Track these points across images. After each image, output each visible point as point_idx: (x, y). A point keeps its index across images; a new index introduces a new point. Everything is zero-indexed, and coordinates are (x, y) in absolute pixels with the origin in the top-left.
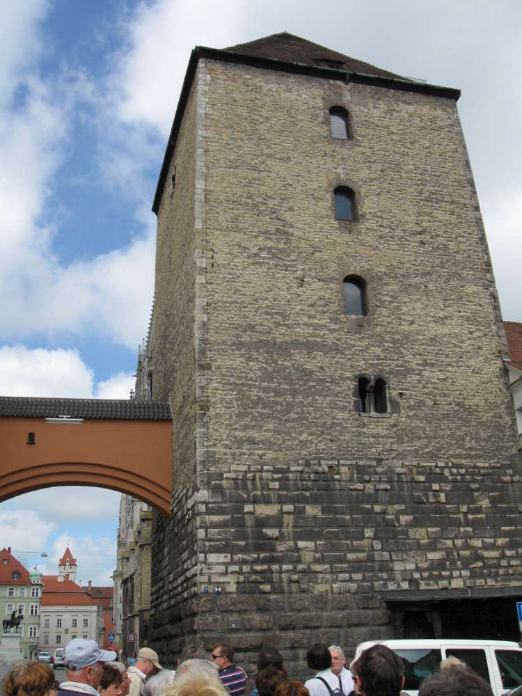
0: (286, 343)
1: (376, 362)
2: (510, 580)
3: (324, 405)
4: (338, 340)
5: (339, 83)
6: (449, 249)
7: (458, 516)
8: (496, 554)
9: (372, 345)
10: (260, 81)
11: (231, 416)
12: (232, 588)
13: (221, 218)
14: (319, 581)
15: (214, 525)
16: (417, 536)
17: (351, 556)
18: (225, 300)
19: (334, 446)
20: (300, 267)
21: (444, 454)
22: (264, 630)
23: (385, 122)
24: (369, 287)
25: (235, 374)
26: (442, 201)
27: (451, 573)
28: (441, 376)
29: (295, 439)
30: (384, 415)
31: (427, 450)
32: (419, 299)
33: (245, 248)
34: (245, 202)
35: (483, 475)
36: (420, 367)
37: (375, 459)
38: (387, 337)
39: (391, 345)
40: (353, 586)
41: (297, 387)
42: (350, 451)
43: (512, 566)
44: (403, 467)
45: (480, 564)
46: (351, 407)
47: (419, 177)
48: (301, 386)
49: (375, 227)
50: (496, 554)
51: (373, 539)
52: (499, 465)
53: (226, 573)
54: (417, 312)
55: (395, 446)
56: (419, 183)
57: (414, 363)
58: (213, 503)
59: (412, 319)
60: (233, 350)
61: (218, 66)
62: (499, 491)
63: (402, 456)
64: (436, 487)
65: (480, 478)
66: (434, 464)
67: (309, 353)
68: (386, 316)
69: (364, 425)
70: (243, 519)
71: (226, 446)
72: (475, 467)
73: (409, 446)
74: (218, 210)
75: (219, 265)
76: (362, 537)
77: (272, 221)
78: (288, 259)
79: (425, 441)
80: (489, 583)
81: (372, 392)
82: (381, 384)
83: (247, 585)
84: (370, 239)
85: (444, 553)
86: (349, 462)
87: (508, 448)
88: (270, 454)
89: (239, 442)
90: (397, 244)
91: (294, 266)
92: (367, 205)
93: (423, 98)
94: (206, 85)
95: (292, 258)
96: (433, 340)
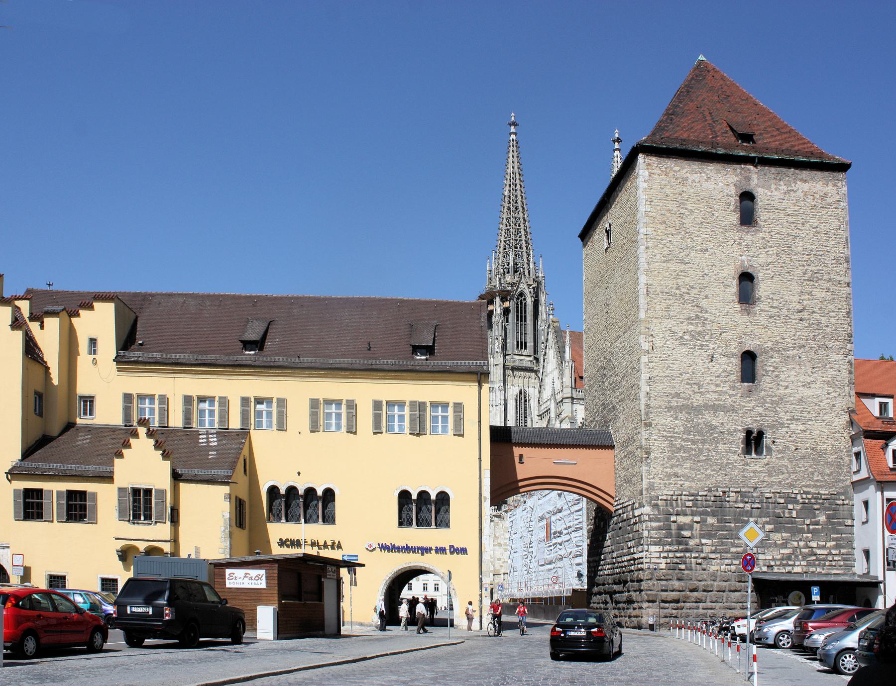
8: (826, 552)
12: (663, 566)
13: (658, 308)
15: (653, 529)
17: (733, 550)
18: (661, 374)
19: (727, 478)
33: (674, 333)
46: (740, 452)
47: (806, 258)
49: (767, 309)
50: (826, 552)
53: (660, 557)
54: (792, 378)
56: (805, 263)
57: (785, 418)
61: (654, 160)
63: (770, 485)
64: (790, 506)
71: (661, 479)
72: (819, 494)
79: (786, 475)
81: (754, 441)
82: (761, 434)
84: (763, 320)
88: (687, 484)
89: (669, 476)
91: (707, 345)
92: (763, 289)
93: (818, 174)
94: (645, 181)
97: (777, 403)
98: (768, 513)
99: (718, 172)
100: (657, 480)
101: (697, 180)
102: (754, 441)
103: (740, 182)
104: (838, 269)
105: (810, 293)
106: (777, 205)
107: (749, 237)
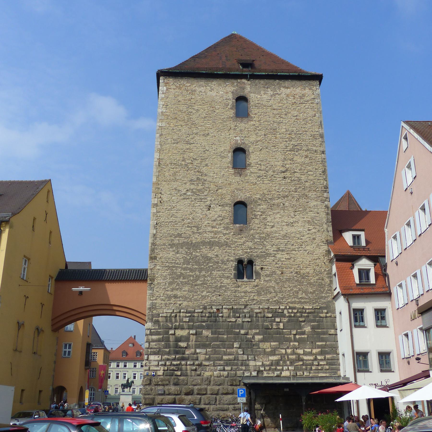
0: (198, 243)
1: (248, 250)
2: (318, 373)
3: (217, 276)
4: (228, 239)
5: (244, 81)
6: (301, 180)
7: (290, 336)
8: (312, 358)
9: (247, 241)
10: (195, 87)
11: (166, 284)
12: (160, 373)
13: (167, 174)
14: (207, 370)
15: (153, 341)
16: (264, 347)
17: (225, 357)
18: (166, 221)
20: (209, 199)
21: (285, 301)
22: (176, 395)
23: (270, 103)
24: (248, 207)
25: (169, 261)
26: (301, 150)
27: (283, 368)
28: (289, 257)
29: (199, 295)
30: (251, 280)
31: (275, 299)
32: (279, 212)
33: (179, 191)
34: (181, 164)
35: (308, 313)
36: (275, 252)
37: (243, 305)
38: (256, 237)
39: (259, 240)
40: (225, 373)
41: (202, 266)
42: (230, 301)
43: (321, 365)
44: (259, 308)
45: (301, 363)
46: (232, 277)
47: (288, 136)
48: (204, 266)
49: (256, 171)
50: (312, 358)
51: (239, 348)
52: (319, 307)
53: (158, 365)
54: (277, 220)
55: (255, 298)
58: (154, 329)
59: (273, 224)
60: (169, 248)
61: (171, 80)
62: (317, 322)
63: (260, 302)
65: (306, 314)
66: (278, 307)
67: (210, 248)
68: (257, 224)
69: (239, 287)
70: (169, 338)
71: (162, 300)
72: (303, 308)
73: (263, 297)
74: (165, 170)
75: (164, 202)
76: (233, 348)
77: (195, 173)
78: (203, 195)
80: (305, 374)
82: (251, 263)
83: (169, 371)
84: (252, 179)
85: (279, 356)
86: (228, 307)
87: (325, 297)
88: (185, 303)
89: (169, 297)
90: (269, 180)
91: (205, 199)
92: (253, 158)
93: (298, 83)
94: (163, 93)
95: (205, 194)
96: (285, 236)
97: (265, 239)
98: (258, 325)
99: (220, 85)
100: (159, 301)
101: (203, 91)
102: (244, 268)
103: (236, 91)
104: (314, 143)
105: (292, 160)
106: (266, 104)
107: (242, 125)
